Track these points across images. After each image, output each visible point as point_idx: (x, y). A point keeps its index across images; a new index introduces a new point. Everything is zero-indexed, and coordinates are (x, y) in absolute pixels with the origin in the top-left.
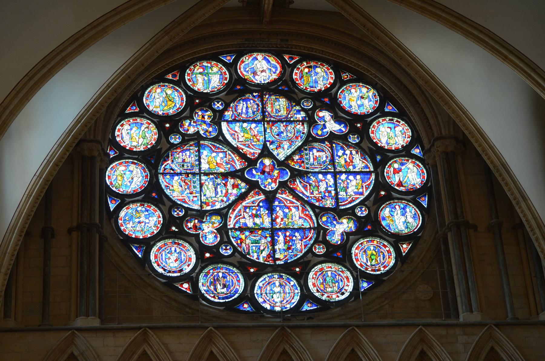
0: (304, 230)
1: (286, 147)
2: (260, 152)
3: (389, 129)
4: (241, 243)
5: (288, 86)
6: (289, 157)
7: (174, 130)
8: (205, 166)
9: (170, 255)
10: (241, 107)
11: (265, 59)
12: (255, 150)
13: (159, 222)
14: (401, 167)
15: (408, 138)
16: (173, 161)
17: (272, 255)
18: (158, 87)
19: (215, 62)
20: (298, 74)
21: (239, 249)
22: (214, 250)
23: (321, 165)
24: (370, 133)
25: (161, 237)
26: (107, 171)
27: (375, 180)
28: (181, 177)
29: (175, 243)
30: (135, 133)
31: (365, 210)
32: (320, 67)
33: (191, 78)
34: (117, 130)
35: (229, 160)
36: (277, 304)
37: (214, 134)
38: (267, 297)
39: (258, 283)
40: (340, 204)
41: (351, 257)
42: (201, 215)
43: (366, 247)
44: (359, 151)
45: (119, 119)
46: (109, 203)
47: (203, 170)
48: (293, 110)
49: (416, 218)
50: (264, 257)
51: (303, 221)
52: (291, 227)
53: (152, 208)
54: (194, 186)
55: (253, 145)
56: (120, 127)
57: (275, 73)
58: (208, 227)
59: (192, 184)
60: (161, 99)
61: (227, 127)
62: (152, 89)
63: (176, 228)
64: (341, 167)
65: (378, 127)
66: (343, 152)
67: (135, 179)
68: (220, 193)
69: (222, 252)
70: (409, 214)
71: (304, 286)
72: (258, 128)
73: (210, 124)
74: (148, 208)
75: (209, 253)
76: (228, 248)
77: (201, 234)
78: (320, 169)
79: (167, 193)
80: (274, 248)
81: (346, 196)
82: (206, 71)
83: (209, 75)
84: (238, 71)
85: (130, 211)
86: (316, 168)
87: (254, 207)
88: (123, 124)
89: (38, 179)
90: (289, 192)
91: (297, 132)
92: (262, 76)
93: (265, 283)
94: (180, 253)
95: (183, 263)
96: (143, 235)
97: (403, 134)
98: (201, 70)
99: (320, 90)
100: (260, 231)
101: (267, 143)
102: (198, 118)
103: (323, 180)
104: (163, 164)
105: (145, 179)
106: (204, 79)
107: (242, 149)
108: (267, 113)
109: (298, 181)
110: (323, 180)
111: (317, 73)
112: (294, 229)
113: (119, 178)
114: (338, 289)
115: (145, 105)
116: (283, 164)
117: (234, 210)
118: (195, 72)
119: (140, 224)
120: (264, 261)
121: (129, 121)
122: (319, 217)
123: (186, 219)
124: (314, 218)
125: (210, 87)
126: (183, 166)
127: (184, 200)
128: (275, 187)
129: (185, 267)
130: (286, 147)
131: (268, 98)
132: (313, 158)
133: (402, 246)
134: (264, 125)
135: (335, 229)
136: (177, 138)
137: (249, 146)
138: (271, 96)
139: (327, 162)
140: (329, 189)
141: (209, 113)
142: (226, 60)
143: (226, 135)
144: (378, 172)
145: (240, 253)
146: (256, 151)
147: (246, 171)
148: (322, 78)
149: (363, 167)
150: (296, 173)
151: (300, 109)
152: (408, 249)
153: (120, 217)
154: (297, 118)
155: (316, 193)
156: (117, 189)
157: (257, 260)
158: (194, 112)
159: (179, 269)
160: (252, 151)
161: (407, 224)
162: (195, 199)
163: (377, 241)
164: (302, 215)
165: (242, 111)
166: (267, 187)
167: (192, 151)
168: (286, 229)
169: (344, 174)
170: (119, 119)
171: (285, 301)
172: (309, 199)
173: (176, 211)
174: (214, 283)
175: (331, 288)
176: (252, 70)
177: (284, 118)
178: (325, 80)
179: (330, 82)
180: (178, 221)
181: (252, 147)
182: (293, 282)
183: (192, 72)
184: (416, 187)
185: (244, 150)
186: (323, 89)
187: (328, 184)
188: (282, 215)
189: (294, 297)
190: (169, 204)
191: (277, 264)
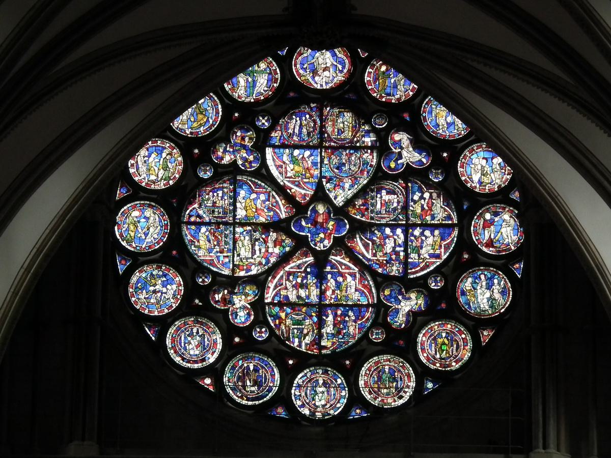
0: (360, 308)
1: (347, 186)
2: (312, 193)
3: (485, 161)
6: (350, 202)
7: (205, 159)
8: (241, 213)
12: (307, 190)
15: (507, 175)
24: (459, 167)
25: (181, 312)
27: (458, 237)
28: (210, 228)
29: (198, 322)
30: (154, 162)
31: (441, 280)
35: (272, 205)
36: (319, 409)
37: (256, 165)
40: (409, 271)
42: (232, 283)
43: (437, 333)
50: (306, 344)
52: (344, 303)
53: (171, 271)
57: (341, 72)
58: (240, 301)
61: (273, 155)
63: (200, 302)
64: (415, 218)
66: (420, 195)
67: (152, 230)
68: (258, 252)
69: (256, 335)
70: (496, 288)
71: (352, 385)
72: (313, 157)
73: (250, 149)
76: (263, 330)
77: (230, 310)
83: (255, 74)
85: (144, 275)
86: (384, 218)
87: (299, 274)
89: (26, 273)
91: (363, 164)
94: (202, 336)
97: (502, 169)
99: (399, 99)
100: (305, 308)
101: (323, 179)
103: (391, 237)
106: (247, 79)
107: (290, 189)
108: (326, 135)
109: (358, 236)
110: (391, 237)
113: (132, 227)
116: (340, 213)
117: (274, 277)
122: (381, 289)
123: (214, 289)
125: (255, 92)
126: (213, 211)
129: (208, 356)
130: (347, 186)
131: (329, 112)
132: (381, 203)
133: (483, 334)
135: (400, 307)
139: (397, 210)
140: (398, 249)
141: (251, 132)
143: (271, 168)
145: (278, 337)
146: (308, 192)
149: (445, 217)
150: (356, 225)
156: (129, 244)
157: (298, 348)
158: (232, 132)
160: (303, 192)
161: (492, 302)
162: (227, 260)
163: (451, 325)
164: (360, 287)
165: (294, 132)
167: (225, 190)
168: (337, 306)
173: (201, 277)
174: (242, 379)
175: (386, 388)
176: (311, 66)
177: (348, 143)
180: (203, 291)
181: (303, 186)
185: (293, 191)
186: (403, 99)
187: (397, 242)
188: (334, 285)
189: (339, 400)
190: (192, 265)
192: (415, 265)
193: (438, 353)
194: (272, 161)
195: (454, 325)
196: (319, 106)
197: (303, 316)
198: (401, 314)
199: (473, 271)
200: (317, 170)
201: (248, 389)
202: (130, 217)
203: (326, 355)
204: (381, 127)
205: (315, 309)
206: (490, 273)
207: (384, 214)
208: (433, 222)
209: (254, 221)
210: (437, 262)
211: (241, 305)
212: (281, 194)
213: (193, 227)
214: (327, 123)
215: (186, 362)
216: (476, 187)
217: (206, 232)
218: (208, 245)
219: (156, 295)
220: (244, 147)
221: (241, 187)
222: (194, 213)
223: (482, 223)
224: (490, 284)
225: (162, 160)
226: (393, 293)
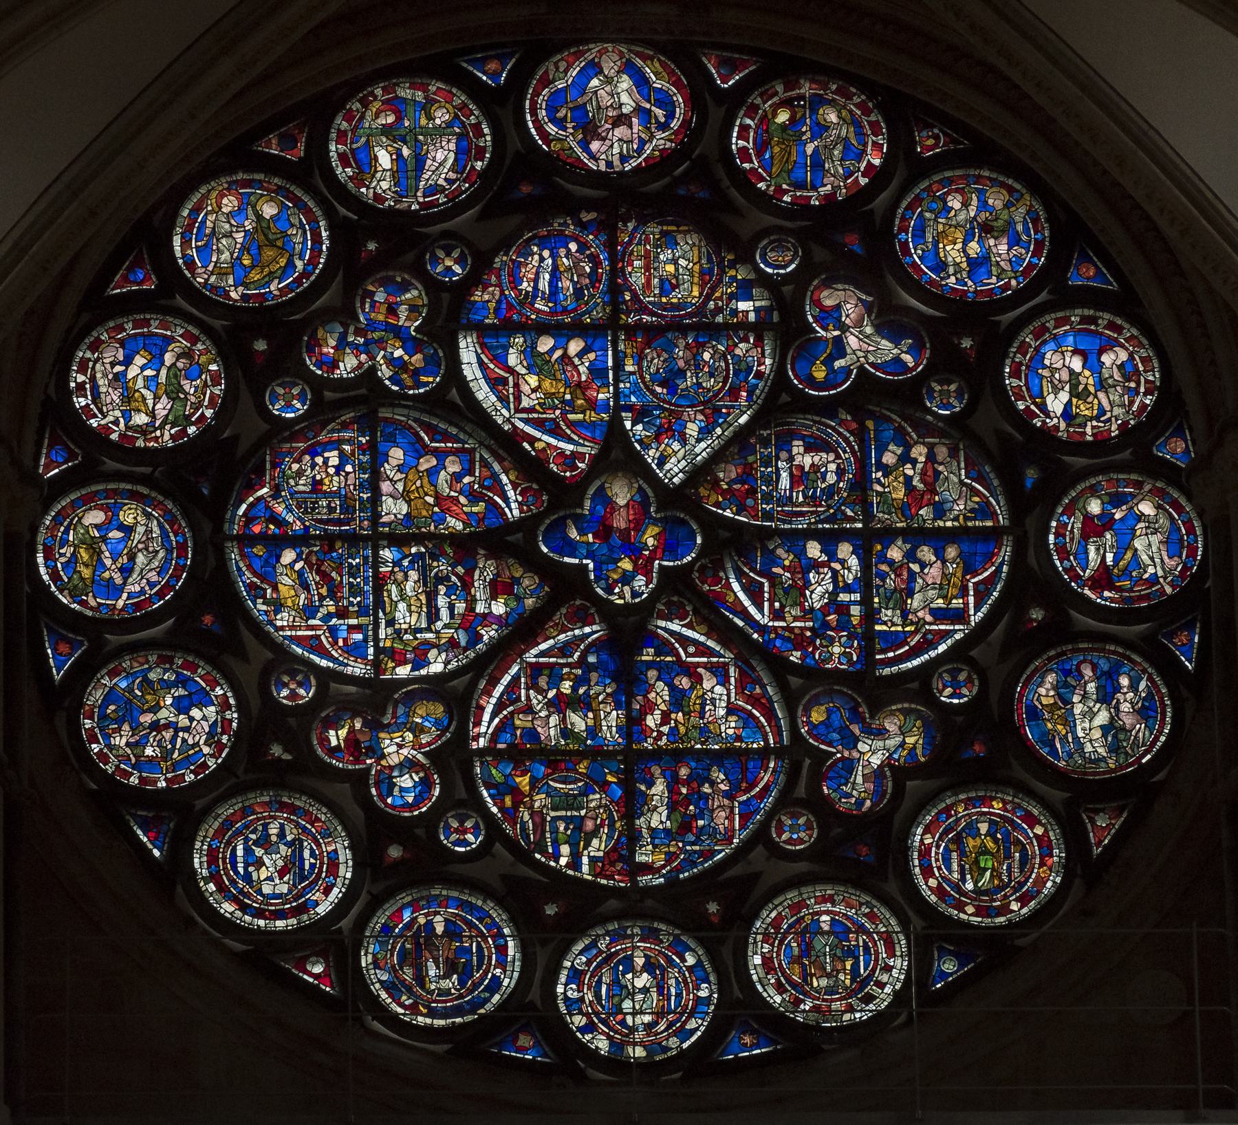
0: (743, 759)
1: (692, 429)
4: (517, 804)
6: (700, 474)
8: (393, 508)
9: (263, 851)
10: (534, 270)
11: (629, 68)
14: (1114, 511)
15: (1145, 394)
16: (276, 493)
17: (624, 852)
18: (228, 189)
23: (816, 506)
25: (233, 780)
27: (1013, 564)
28: (306, 551)
29: (283, 807)
31: (969, 680)
32: (834, 100)
33: (353, 151)
35: (481, 486)
37: (431, 379)
40: (878, 657)
41: (907, 860)
45: (85, 317)
47: (384, 525)
49: (1153, 714)
52: (699, 746)
55: (571, 424)
56: (88, 355)
57: (663, 127)
58: (400, 746)
60: (239, 237)
61: (479, 351)
62: (205, 197)
63: (286, 750)
64: (890, 513)
65: (1037, 349)
67: (141, 559)
68: (444, 614)
72: (592, 356)
73: (414, 338)
75: (400, 844)
76: (469, 824)
77: (373, 772)
78: (813, 520)
80: (634, 824)
87: (565, 670)
90: (696, 612)
91: (736, 373)
92: (615, 139)
93: (596, 956)
94: (296, 845)
96: (169, 776)
97: (1129, 380)
98: (391, 119)
99: (830, 197)
101: (623, 414)
103: (823, 565)
105: (178, 557)
107: (532, 440)
109: (729, 565)
110: (823, 565)
111: (820, 129)
113: (84, 555)
114: (853, 981)
115: (180, 261)
117: (494, 682)
118: (367, 125)
119: (159, 732)
120: (596, 876)
122: (801, 708)
127: (314, 643)
129: (314, 898)
130: (692, 429)
132: (791, 475)
133: (1093, 822)
135: (855, 755)
136: (293, 397)
138: (645, 224)
140: (843, 597)
141: (415, 293)
142: (484, 73)
144: (1026, 532)
145: (511, 844)
146: (581, 449)
147: (542, 528)
148: (840, 147)
149: (972, 511)
150: (723, 534)
151: (752, 276)
152: (1113, 831)
153: (87, 708)
157: (570, 872)
158: (360, 292)
159: (294, 904)
161: (1115, 737)
162: (359, 637)
165: (536, 288)
166: (617, 590)
167: (347, 448)
170: (85, 317)
171: (662, 1026)
173: (286, 685)
175: (828, 976)
176: (577, 113)
177: (690, 315)
178: (852, 155)
180: (292, 721)
181: (568, 432)
183: (356, 127)
184: (1163, 592)
187: (840, 579)
192: (895, 640)
193: (968, 877)
194: (475, 366)
195: (1012, 802)
197: (580, 784)
198: (860, 773)
199: (1059, 655)
200: (606, 390)
201: (433, 987)
202: (79, 526)
203: (649, 890)
204: (782, 271)
206: (1108, 658)
207: (801, 505)
208: (941, 524)
210: (956, 631)
211: (402, 758)
212: (504, 455)
213: (259, 550)
215: (253, 916)
216: (1056, 428)
217: (295, 561)
218: (303, 596)
220: (399, 333)
222: (260, 510)
225: (164, 372)
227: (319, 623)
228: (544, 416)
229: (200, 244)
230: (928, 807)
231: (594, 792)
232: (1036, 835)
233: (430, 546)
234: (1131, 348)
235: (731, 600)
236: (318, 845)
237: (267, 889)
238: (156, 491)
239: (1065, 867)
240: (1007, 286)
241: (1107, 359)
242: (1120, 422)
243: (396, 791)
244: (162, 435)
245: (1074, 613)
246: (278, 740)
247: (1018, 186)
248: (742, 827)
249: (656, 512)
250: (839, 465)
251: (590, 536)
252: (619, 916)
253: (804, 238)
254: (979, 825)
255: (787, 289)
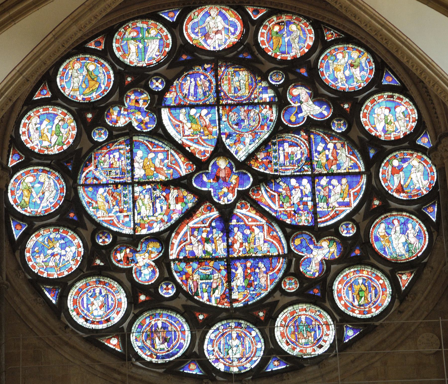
1: (247, 141)
2: (212, 150)
3: (387, 111)
4: (187, 279)
5: (252, 53)
6: (252, 156)
8: (139, 173)
10: (188, 86)
11: (220, 14)
13: (79, 253)
14: (403, 164)
15: (412, 122)
16: (96, 167)
17: (227, 295)
18: (77, 61)
19: (153, 22)
20: (265, 35)
21: (185, 288)
22: (151, 290)
25: (82, 273)
26: (10, 184)
28: (107, 189)
29: (100, 282)
31: (353, 227)
32: (294, 22)
33: (122, 46)
34: (21, 126)
37: (152, 126)
38: (220, 353)
39: (209, 334)
40: (319, 220)
44: (346, 143)
45: (25, 108)
46: (13, 229)
47: (136, 179)
48: (258, 87)
50: (216, 298)
51: (269, 246)
52: (254, 255)
53: (69, 233)
54: (124, 201)
55: (203, 140)
56: (27, 121)
57: (233, 34)
58: (144, 259)
59: (122, 198)
60: (81, 78)
61: (169, 115)
62: (68, 64)
63: (101, 262)
64: (321, 168)
65: (372, 108)
66: (324, 145)
67: (47, 194)
68: (159, 210)
69: (162, 292)
70: (411, 233)
72: (210, 115)
73: (145, 111)
74: (65, 235)
76: (170, 286)
77: (134, 269)
78: (293, 172)
79: (89, 212)
80: (231, 285)
81: (328, 208)
82: (141, 35)
84: (183, 33)
85: (40, 239)
86: (288, 169)
87: (204, 229)
88: (30, 115)
90: (251, 206)
91: (263, 120)
93: (218, 334)
94: (106, 296)
95: (110, 310)
96: (58, 273)
97: (406, 117)
98: (135, 34)
100: (212, 262)
102: (130, 104)
103: (297, 187)
104: (84, 172)
105: (60, 193)
106: (138, 47)
108: (222, 94)
109: (262, 189)
110: (297, 187)
111: (290, 33)
112: (257, 257)
113: (26, 193)
114: (314, 339)
115: (60, 87)
117: (178, 234)
118: (126, 36)
119: (54, 257)
120: (217, 304)
121: (38, 111)
122: (291, 240)
124: (284, 241)
125: (147, 57)
127: (111, 222)
128: (233, 199)
129: (113, 316)
130: (247, 141)
131: (223, 72)
132: (284, 155)
133: (401, 278)
134: (218, 111)
137: (198, 141)
138: (228, 68)
140: (305, 199)
141: (145, 95)
143: (167, 128)
144: (371, 173)
145: (186, 294)
146: (207, 149)
147: (194, 178)
148: (297, 39)
149: (351, 166)
150: (260, 178)
151: (267, 85)
152: (409, 281)
153: (27, 249)
154: (264, 99)
155: (287, 205)
156: (24, 209)
157: (208, 303)
158: (125, 95)
159: (106, 319)
160: (202, 149)
161: (408, 246)
162: (127, 219)
163: (367, 271)
164: (269, 239)
165: (189, 92)
166: (222, 199)
167: (122, 151)
168: (246, 258)
169: (325, 178)
170: (25, 108)
172: (277, 215)
173: (101, 238)
175: (305, 338)
176: (202, 30)
177: (245, 100)
178: (302, 41)
179: (308, 45)
180: (104, 251)
181: (202, 143)
182: (255, 332)
183: (123, 38)
184: (423, 193)
185: (192, 148)
186: (298, 56)
187: (303, 192)
188: (241, 238)
189: (256, 352)
191: (234, 307)
192: (325, 214)
196: (213, 66)
197: (211, 270)
199: (385, 217)
202: (24, 183)
203: (237, 309)
205: (223, 263)
208: (339, 171)
209: (154, 179)
213: (90, 189)
214: (223, 82)
215: (90, 324)
219: (54, 258)
220: (139, 109)
221: (138, 148)
222: (90, 175)
223: (390, 170)
224: (405, 229)
225: (54, 126)
226: (304, 243)
227: (113, 215)
228: (193, 138)
229: (66, 80)
230: (340, 274)
231: (216, 273)
232: (381, 284)
233: (153, 185)
234: (406, 106)
235: (264, 201)
236: (114, 296)
237: (95, 313)
238: (52, 169)
239: (391, 295)
240: (360, 86)
241: (398, 110)
242: (403, 133)
243: (143, 275)
244: (54, 149)
245: (390, 202)
246: (99, 259)
247: (362, 50)
248: (271, 284)
249: (236, 170)
250: (301, 152)
251: (212, 180)
252: (226, 319)
253: (285, 71)
254: (359, 280)
255: (280, 90)
